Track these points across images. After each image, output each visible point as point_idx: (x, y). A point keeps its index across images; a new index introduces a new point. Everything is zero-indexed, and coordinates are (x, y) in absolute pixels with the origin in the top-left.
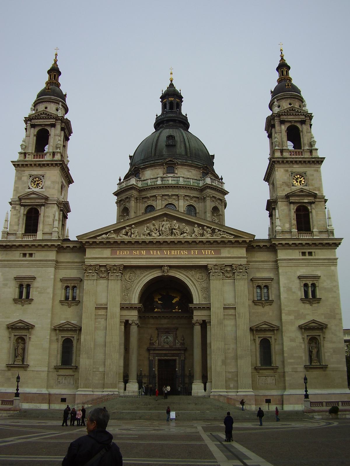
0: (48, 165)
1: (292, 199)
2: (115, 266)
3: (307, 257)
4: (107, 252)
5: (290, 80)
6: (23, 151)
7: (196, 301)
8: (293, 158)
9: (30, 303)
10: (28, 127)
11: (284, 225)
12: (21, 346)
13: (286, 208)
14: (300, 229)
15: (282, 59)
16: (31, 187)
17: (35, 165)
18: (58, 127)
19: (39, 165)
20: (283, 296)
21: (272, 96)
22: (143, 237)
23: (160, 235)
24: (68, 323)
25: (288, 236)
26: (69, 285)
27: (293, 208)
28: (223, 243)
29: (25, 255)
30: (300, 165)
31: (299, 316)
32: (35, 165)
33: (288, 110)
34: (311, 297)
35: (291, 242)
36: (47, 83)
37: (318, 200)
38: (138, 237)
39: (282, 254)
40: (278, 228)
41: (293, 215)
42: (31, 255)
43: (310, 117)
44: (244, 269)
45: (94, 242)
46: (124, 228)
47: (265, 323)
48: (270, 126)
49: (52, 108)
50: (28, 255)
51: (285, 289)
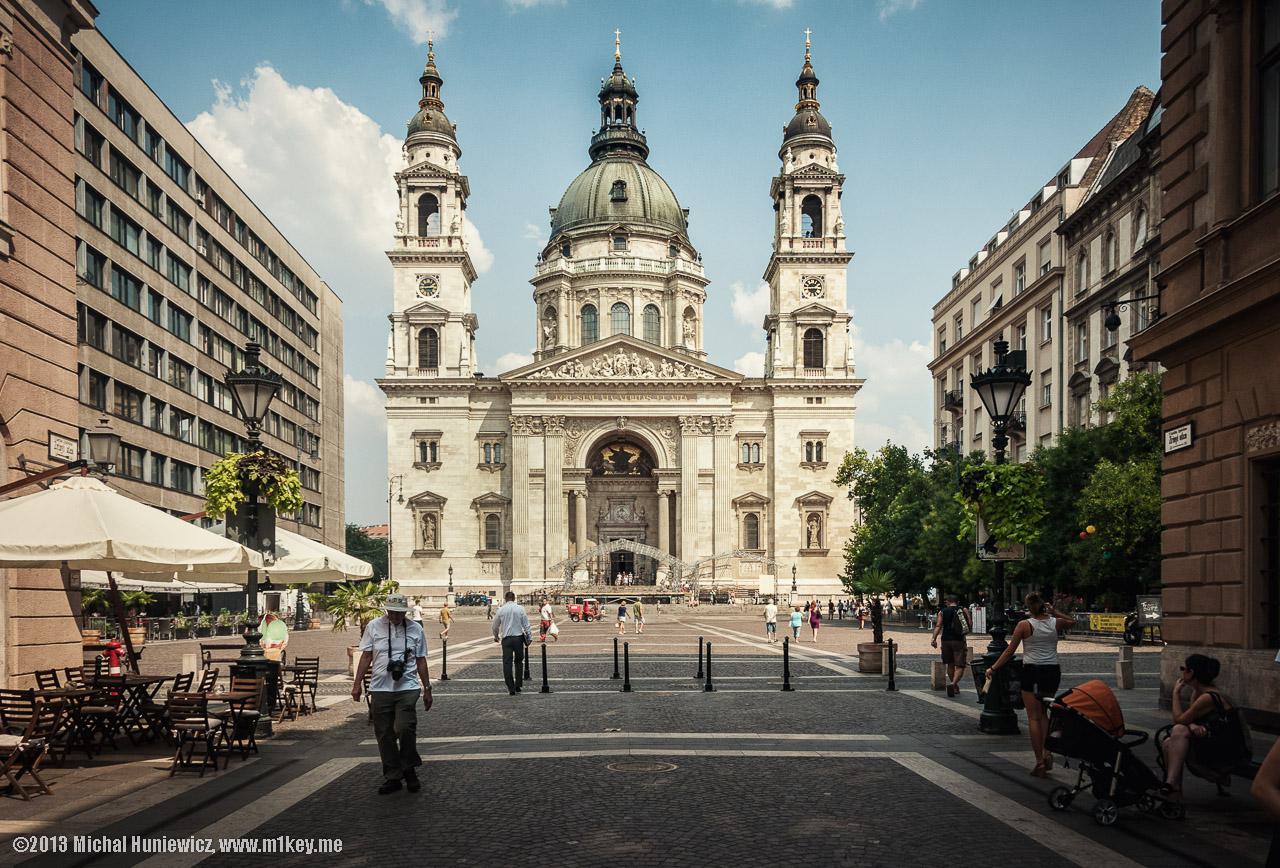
0: (443, 258)
1: (800, 320)
2: (553, 417)
3: (814, 405)
4: (541, 400)
5: (816, 107)
6: (402, 235)
7: (662, 465)
8: (807, 254)
9: (438, 469)
10: (404, 191)
11: (786, 359)
14: (807, 364)
15: (807, 64)
16: (421, 295)
17: (423, 258)
18: (451, 190)
19: (430, 258)
21: (787, 138)
22: (591, 377)
24: (493, 495)
25: (789, 375)
26: (490, 442)
27: (801, 332)
28: (701, 387)
30: (816, 264)
31: (798, 485)
32: (423, 258)
33: (807, 169)
34: (815, 460)
37: (837, 320)
38: (584, 377)
39: (780, 401)
40: (776, 363)
41: (801, 343)
42: (432, 400)
44: (727, 422)
45: (522, 384)
46: (564, 363)
47: (753, 495)
48: (778, 194)
49: (437, 156)
50: (428, 400)
51: (781, 449)
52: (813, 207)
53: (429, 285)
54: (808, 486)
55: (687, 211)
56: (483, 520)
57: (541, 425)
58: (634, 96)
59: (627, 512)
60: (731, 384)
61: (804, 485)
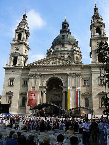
4: (36, 70)
7: (64, 85)
12: (10, 99)
13: (94, 54)
14: (99, 61)
20: (93, 83)
23: (52, 64)
29: (12, 71)
31: (98, 90)
35: (96, 65)
36: (23, 20)
42: (14, 71)
43: (104, 24)
46: (41, 62)
48: (91, 28)
52: (99, 31)
53: (17, 49)
54: (101, 90)
55: (78, 42)
56: (22, 98)
57: (35, 76)
58: (68, 24)
59: (58, 98)
60: (80, 65)
61: (100, 90)
